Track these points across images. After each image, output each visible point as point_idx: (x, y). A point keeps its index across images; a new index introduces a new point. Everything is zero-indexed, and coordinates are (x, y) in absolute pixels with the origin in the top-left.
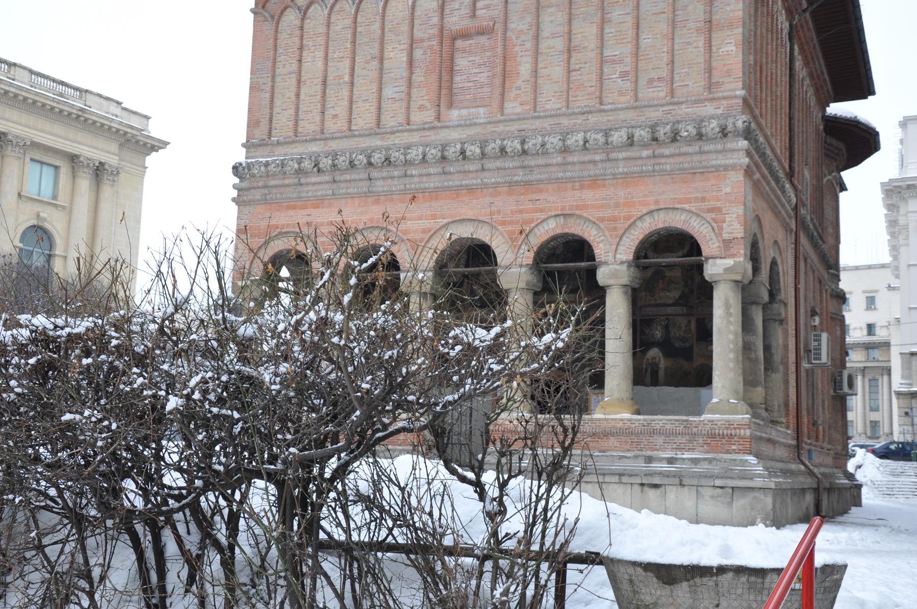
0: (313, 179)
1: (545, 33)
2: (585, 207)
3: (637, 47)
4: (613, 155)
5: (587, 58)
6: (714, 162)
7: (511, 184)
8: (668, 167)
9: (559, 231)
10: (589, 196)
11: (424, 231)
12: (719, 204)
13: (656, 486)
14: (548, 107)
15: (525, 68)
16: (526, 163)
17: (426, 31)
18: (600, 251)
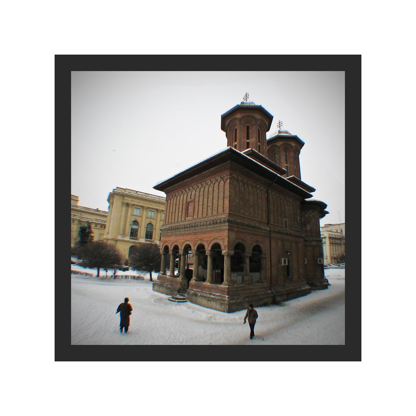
0: (169, 232)
1: (200, 201)
2: (203, 238)
3: (213, 203)
4: (207, 227)
5: (205, 206)
6: (222, 228)
7: (194, 233)
8: (215, 229)
9: (200, 243)
10: (204, 235)
11: (182, 242)
12: (224, 238)
13: (210, 301)
14: (200, 216)
15: (197, 209)
16: (195, 229)
17: (185, 202)
18: (206, 247)
